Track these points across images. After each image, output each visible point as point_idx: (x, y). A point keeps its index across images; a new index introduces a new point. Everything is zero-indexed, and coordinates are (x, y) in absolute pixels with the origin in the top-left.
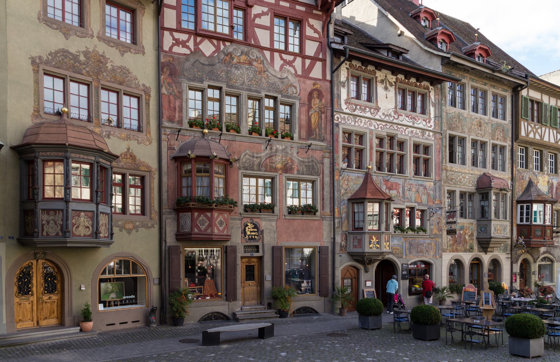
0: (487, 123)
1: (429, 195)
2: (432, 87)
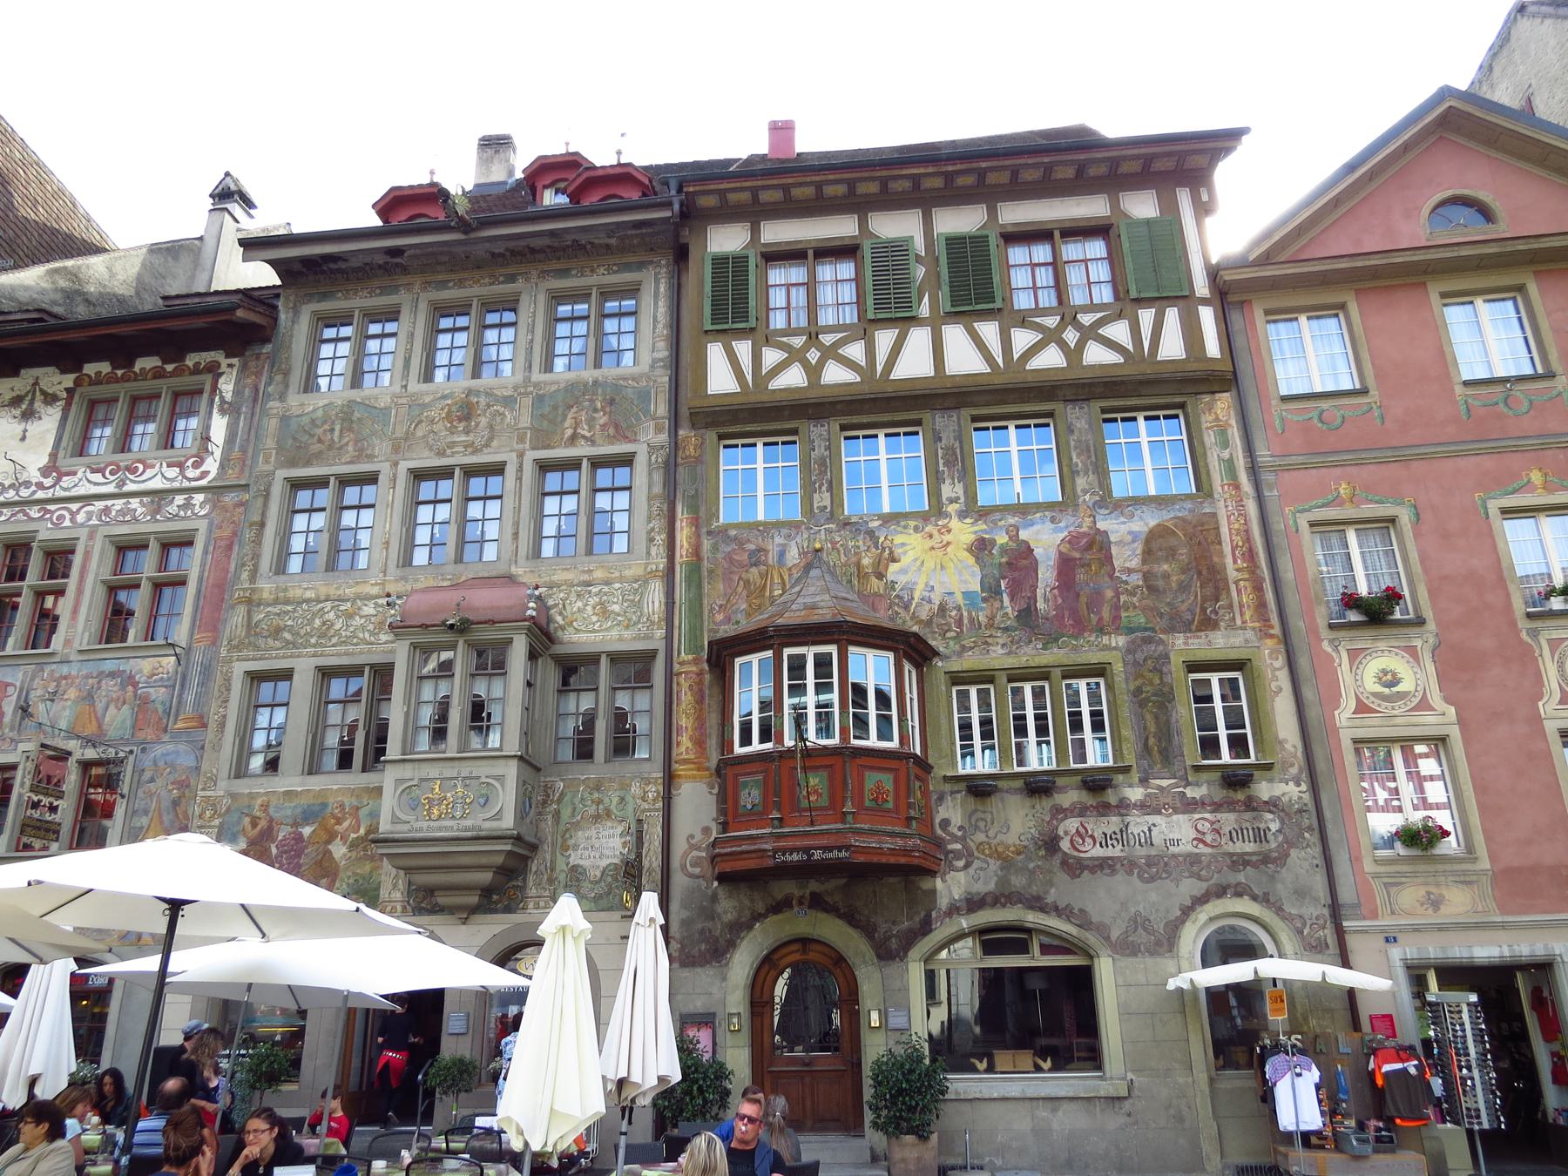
0: (508, 401)
1: (143, 703)
2: (235, 361)
